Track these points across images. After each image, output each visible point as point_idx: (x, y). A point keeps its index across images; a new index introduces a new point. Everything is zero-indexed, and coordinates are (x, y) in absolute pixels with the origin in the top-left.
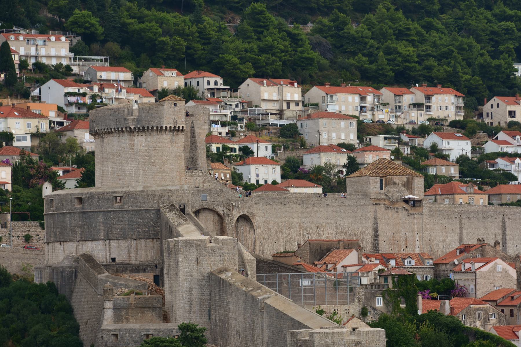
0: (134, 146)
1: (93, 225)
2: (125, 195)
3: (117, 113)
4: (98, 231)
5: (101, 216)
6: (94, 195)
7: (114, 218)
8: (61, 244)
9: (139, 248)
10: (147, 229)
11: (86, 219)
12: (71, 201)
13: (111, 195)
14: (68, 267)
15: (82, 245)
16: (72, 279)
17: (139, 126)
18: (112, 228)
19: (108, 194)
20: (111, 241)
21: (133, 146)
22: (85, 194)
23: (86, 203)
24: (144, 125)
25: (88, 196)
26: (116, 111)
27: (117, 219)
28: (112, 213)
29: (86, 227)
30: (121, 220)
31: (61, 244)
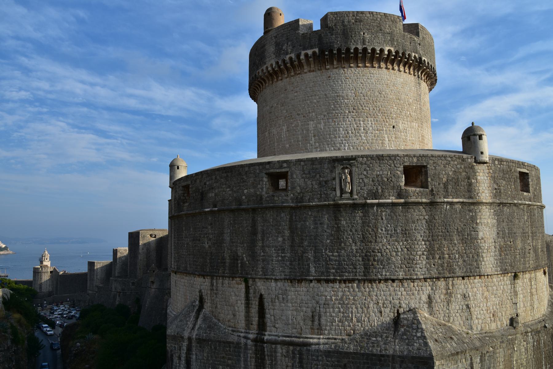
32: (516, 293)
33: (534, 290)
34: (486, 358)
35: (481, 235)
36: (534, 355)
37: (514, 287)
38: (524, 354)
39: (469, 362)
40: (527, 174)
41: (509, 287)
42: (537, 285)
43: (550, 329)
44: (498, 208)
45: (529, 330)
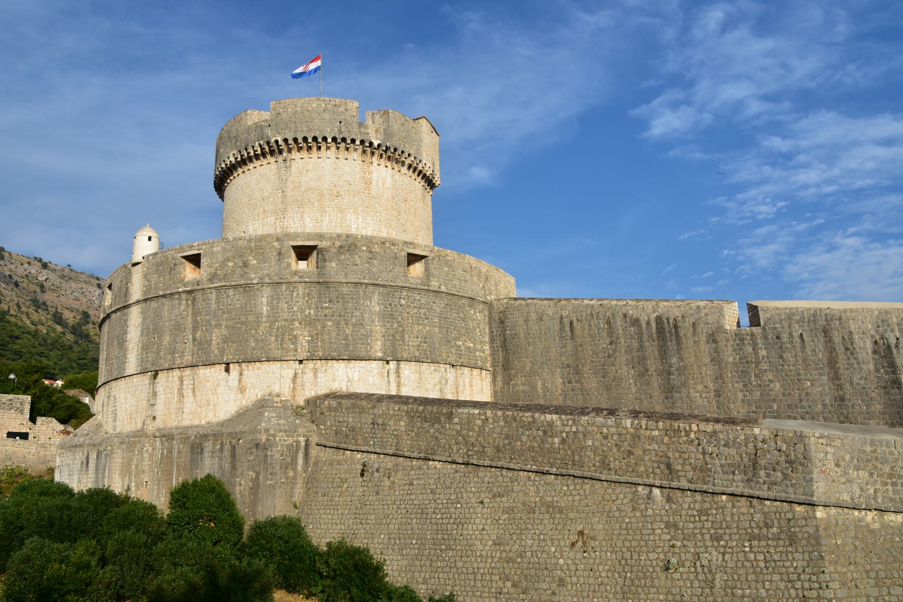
0: (371, 183)
1: (354, 320)
2: (432, 255)
3: (342, 109)
4: (367, 336)
5: (376, 297)
6: (358, 244)
7: (409, 307)
8: (227, 370)
9: (461, 388)
10: (472, 345)
11: (330, 301)
12: (280, 254)
13: (402, 250)
14: (285, 431)
15: (315, 371)
16: (295, 470)
17: (388, 144)
18: (404, 331)
19: (393, 245)
20: (402, 364)
21: (368, 183)
22: (331, 238)
23: (331, 261)
24: (397, 146)
25: (338, 244)
26: (340, 106)
27: (415, 311)
28: (404, 294)
29: (330, 323)
30: (425, 314)
31: (227, 370)
32: (155, 394)
33: (188, 392)
34: (103, 456)
35: (129, 336)
36: (160, 464)
37: (153, 387)
38: (147, 460)
39: (85, 457)
40: (199, 255)
41: (148, 387)
42: (196, 383)
43: (189, 438)
44: (144, 305)
45: (157, 434)
